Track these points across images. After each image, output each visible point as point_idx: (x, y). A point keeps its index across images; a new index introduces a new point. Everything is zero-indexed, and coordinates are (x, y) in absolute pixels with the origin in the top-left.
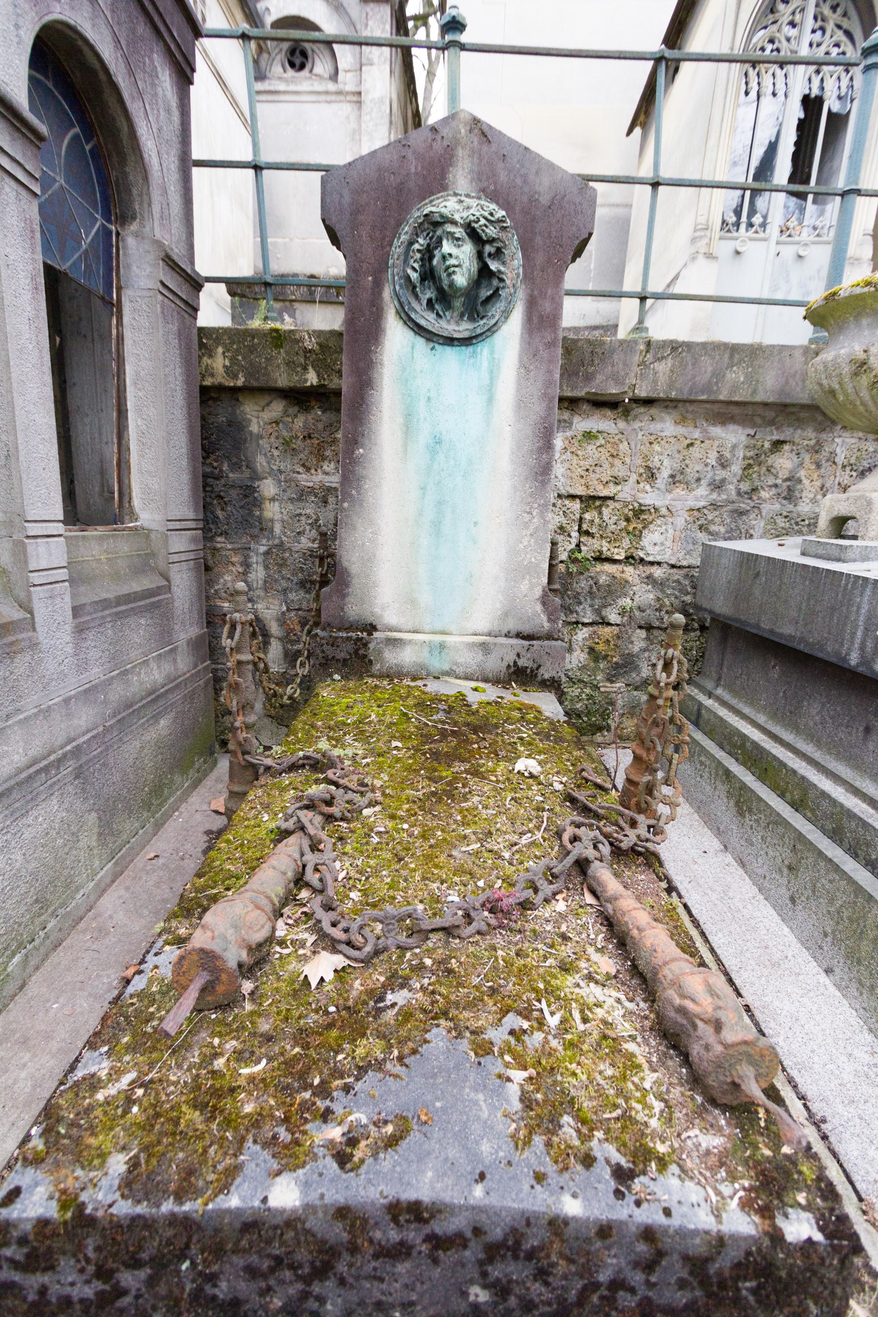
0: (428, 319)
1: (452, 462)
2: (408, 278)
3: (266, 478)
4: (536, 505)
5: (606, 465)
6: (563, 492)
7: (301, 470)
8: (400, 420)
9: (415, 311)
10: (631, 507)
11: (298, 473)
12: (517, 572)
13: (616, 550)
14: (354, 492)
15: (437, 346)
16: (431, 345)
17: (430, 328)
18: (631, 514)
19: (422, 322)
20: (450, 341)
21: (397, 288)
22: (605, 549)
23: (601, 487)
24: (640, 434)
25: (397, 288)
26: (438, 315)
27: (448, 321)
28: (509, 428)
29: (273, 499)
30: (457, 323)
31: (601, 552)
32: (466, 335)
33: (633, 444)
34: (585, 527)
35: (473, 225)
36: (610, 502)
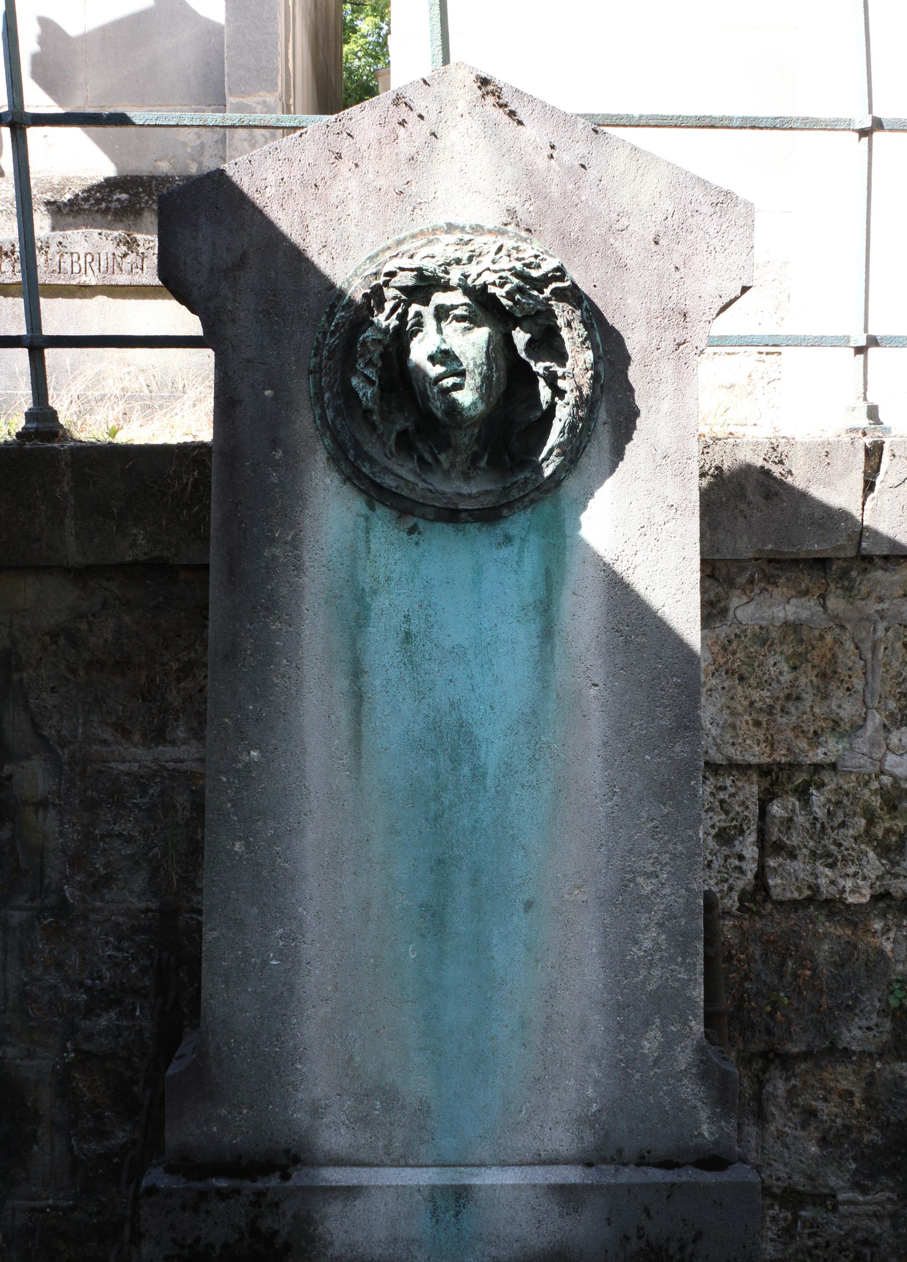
0: (402, 473)
1: (466, 770)
2: (350, 394)
3: (27, 757)
4: (666, 858)
5: (808, 698)
6: (719, 759)
7: (108, 735)
8: (342, 684)
9: (372, 461)
10: (875, 785)
11: (105, 742)
12: (630, 1009)
13: (849, 884)
14: (238, 847)
15: (422, 524)
16: (410, 521)
17: (405, 492)
18: (876, 802)
19: (389, 482)
20: (451, 515)
21: (330, 414)
22: (822, 881)
23: (803, 744)
24: (881, 626)
25: (330, 414)
26: (422, 461)
27: (446, 474)
28: (593, 691)
29: (42, 804)
30: (466, 477)
31: (815, 888)
32: (488, 502)
33: (867, 646)
34: (775, 834)
35: (492, 289)
36: (826, 776)
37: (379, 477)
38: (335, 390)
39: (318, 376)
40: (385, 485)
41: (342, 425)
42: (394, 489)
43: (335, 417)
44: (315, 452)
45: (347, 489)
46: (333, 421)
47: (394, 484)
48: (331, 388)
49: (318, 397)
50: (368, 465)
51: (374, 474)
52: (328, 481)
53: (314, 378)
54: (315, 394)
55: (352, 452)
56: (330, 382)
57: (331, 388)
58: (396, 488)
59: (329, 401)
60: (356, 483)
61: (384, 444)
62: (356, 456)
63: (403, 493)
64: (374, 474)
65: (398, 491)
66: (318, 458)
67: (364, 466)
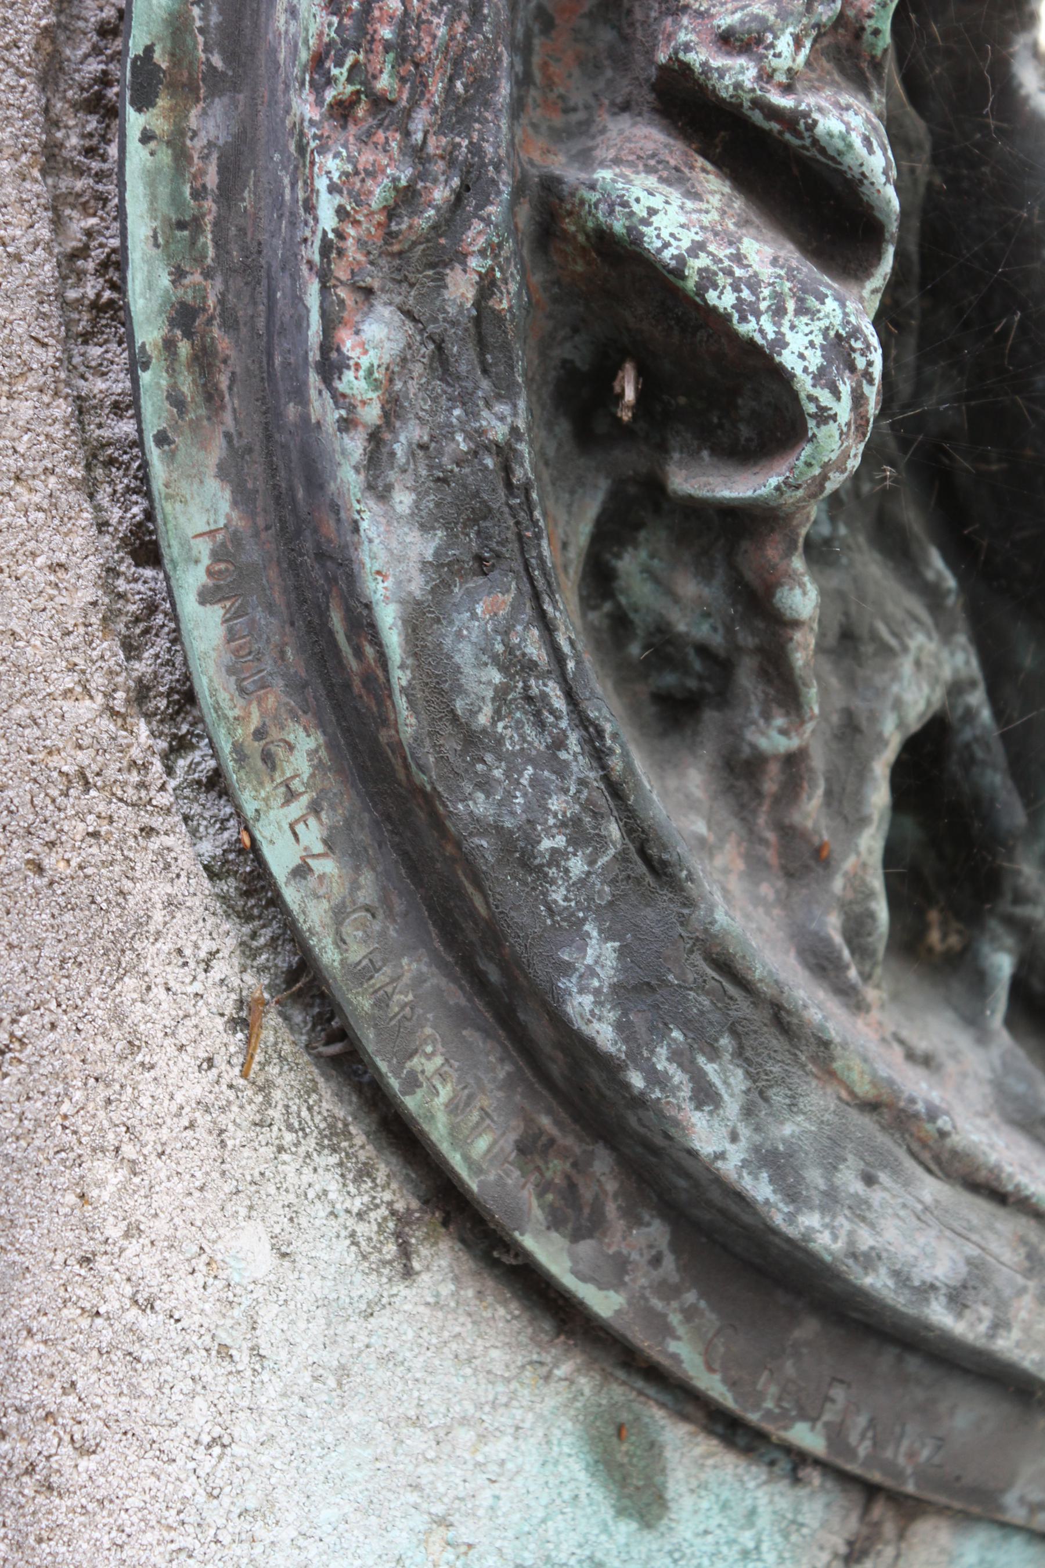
37: (831, 1201)
38: (461, 288)
39: (210, 124)
40: (877, 1282)
41: (515, 664)
42: (939, 1315)
43: (444, 573)
44: (119, 957)
45: (441, 1325)
46: (420, 620)
47: (941, 1262)
48: (414, 260)
49: (204, 360)
50: (729, 1079)
51: (774, 1161)
52: (248, 1249)
53: (177, 143)
54: (184, 317)
55: (599, 955)
56: (407, 197)
57: (414, 260)
58: (958, 1298)
59: (393, 409)
60: (551, 1254)
61: (801, 861)
62: (639, 990)
63: (1006, 1345)
64: (774, 1161)
65: (964, 1327)
66: (151, 1016)
67: (705, 1096)
